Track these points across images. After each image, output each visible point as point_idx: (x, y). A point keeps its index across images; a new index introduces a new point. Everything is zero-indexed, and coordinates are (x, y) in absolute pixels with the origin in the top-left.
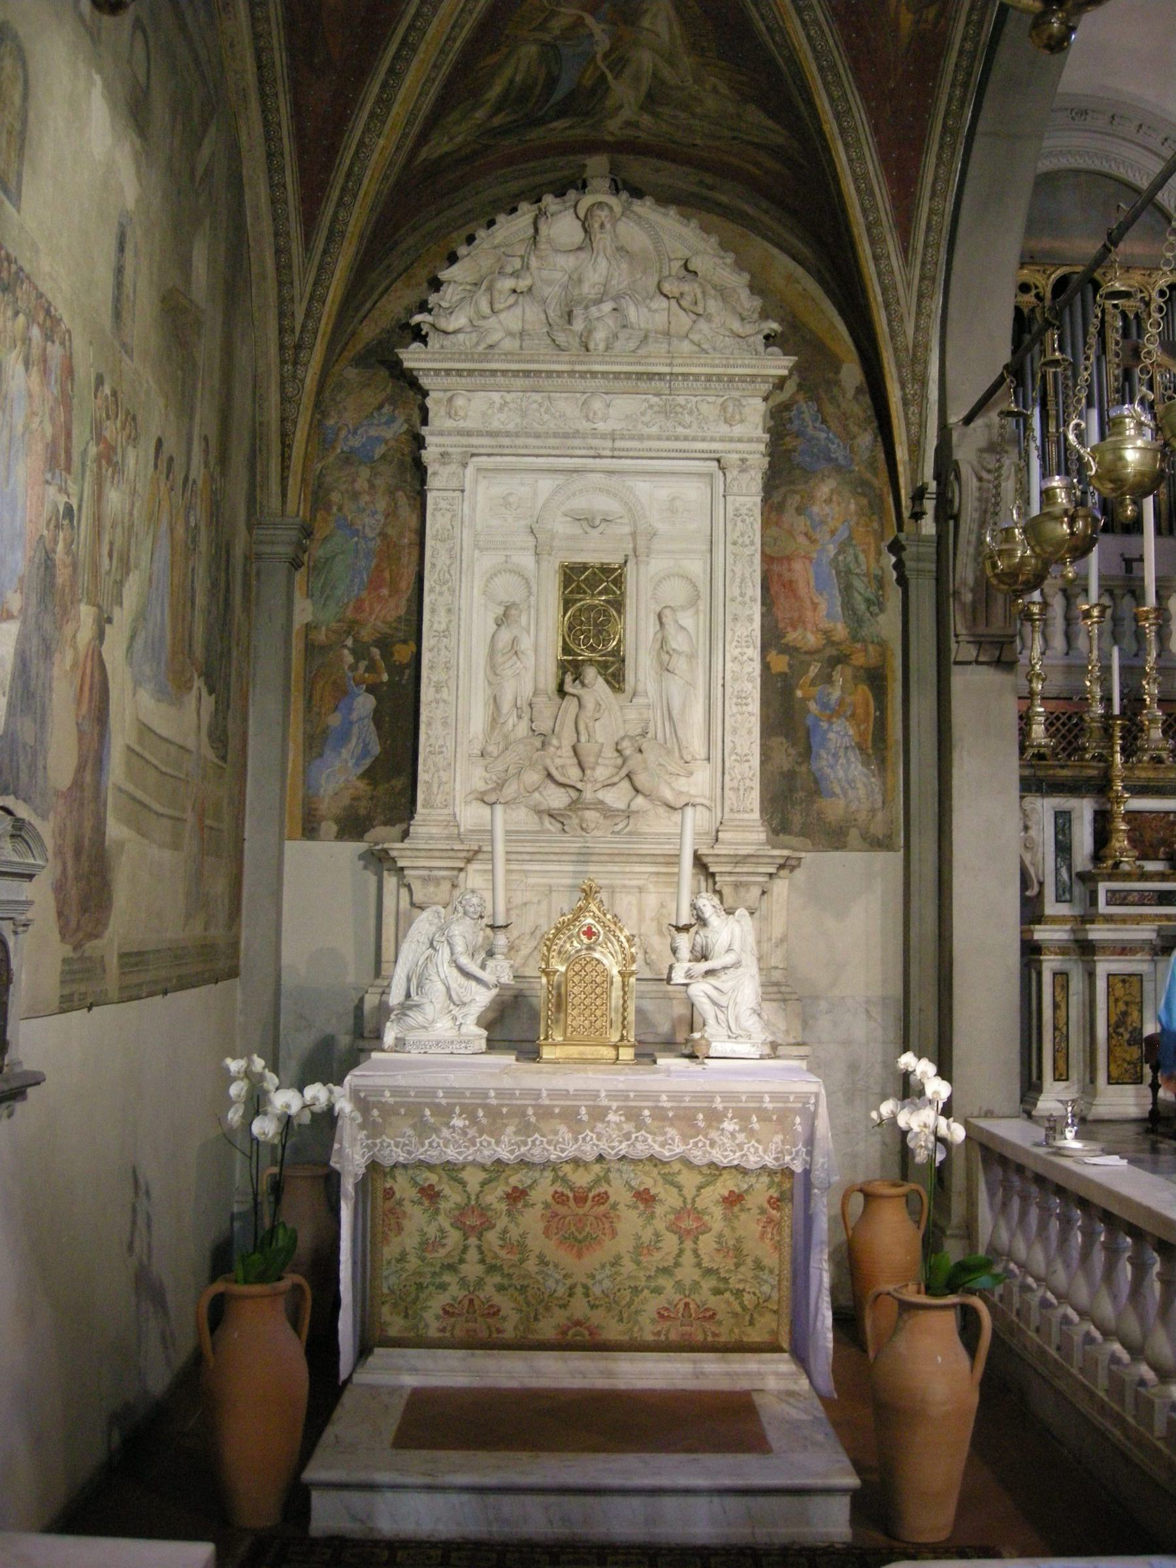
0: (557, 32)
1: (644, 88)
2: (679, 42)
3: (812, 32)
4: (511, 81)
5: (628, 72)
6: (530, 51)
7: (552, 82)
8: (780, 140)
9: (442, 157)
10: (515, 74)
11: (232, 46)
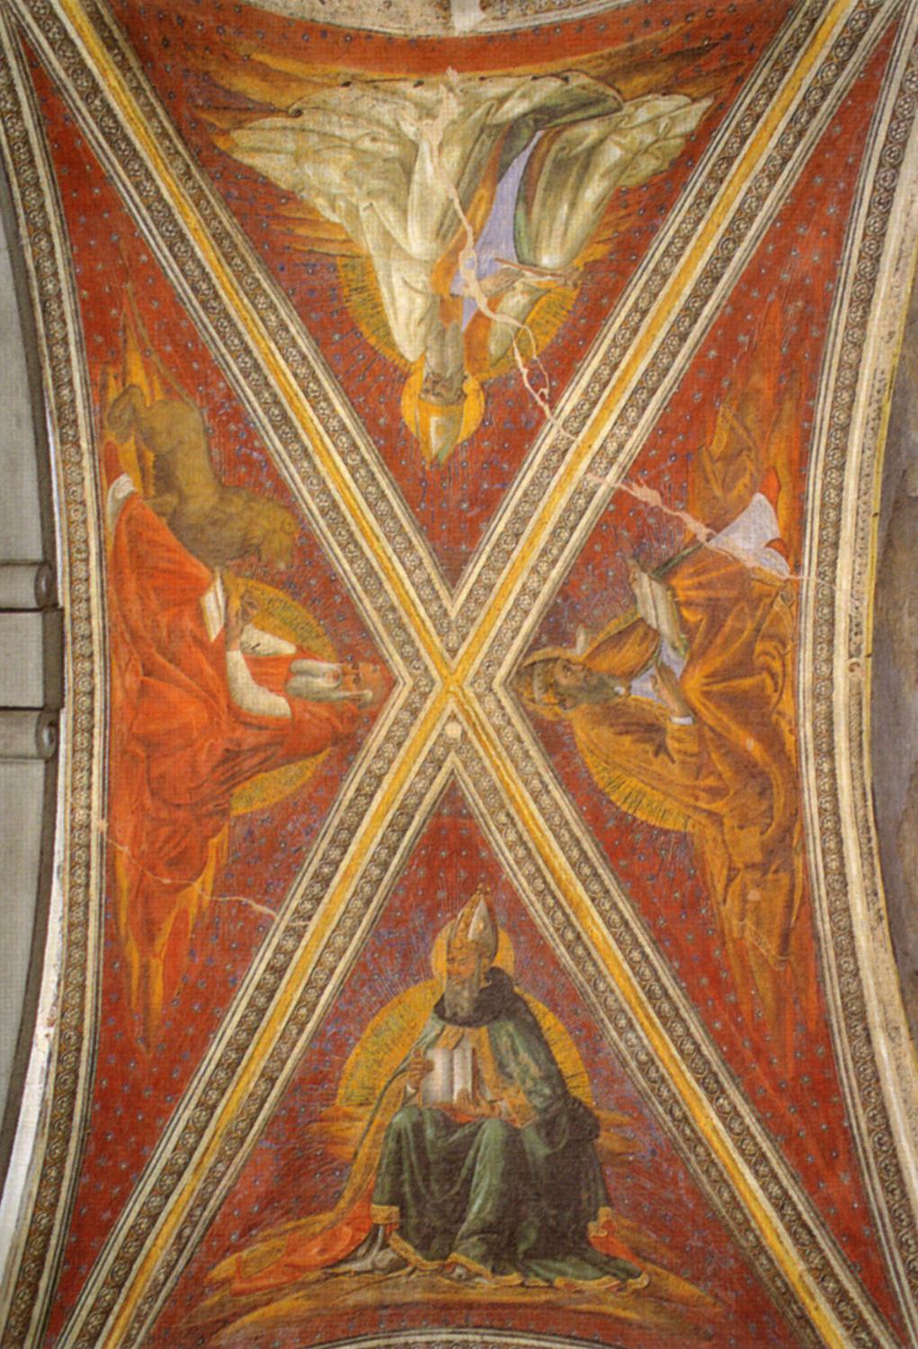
0: (518, 285)
1: (415, 188)
2: (381, 275)
3: (236, 342)
4: (573, 205)
5: (436, 214)
6: (549, 259)
7: (525, 197)
8: (243, 138)
9: (667, 91)
10: (567, 224)
11: (891, 334)
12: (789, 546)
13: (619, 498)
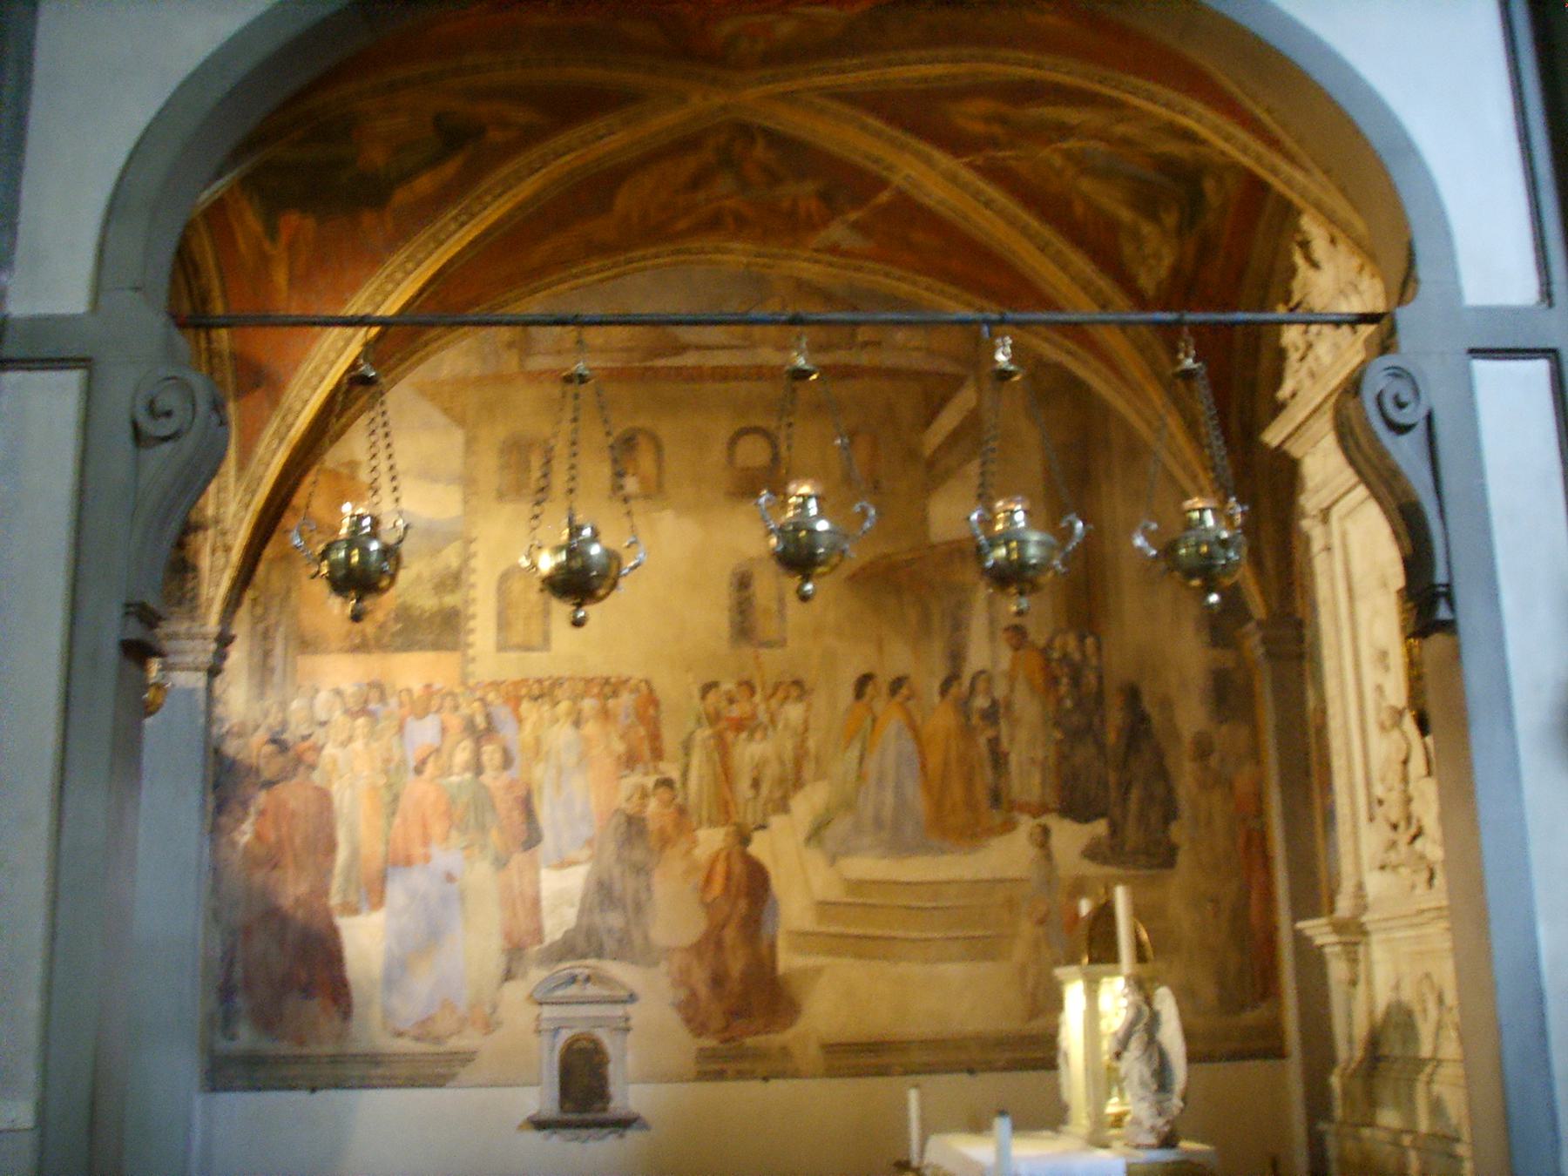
6: (1086, 185)
9: (1175, 271)
12: (834, 249)
13: (881, 184)
